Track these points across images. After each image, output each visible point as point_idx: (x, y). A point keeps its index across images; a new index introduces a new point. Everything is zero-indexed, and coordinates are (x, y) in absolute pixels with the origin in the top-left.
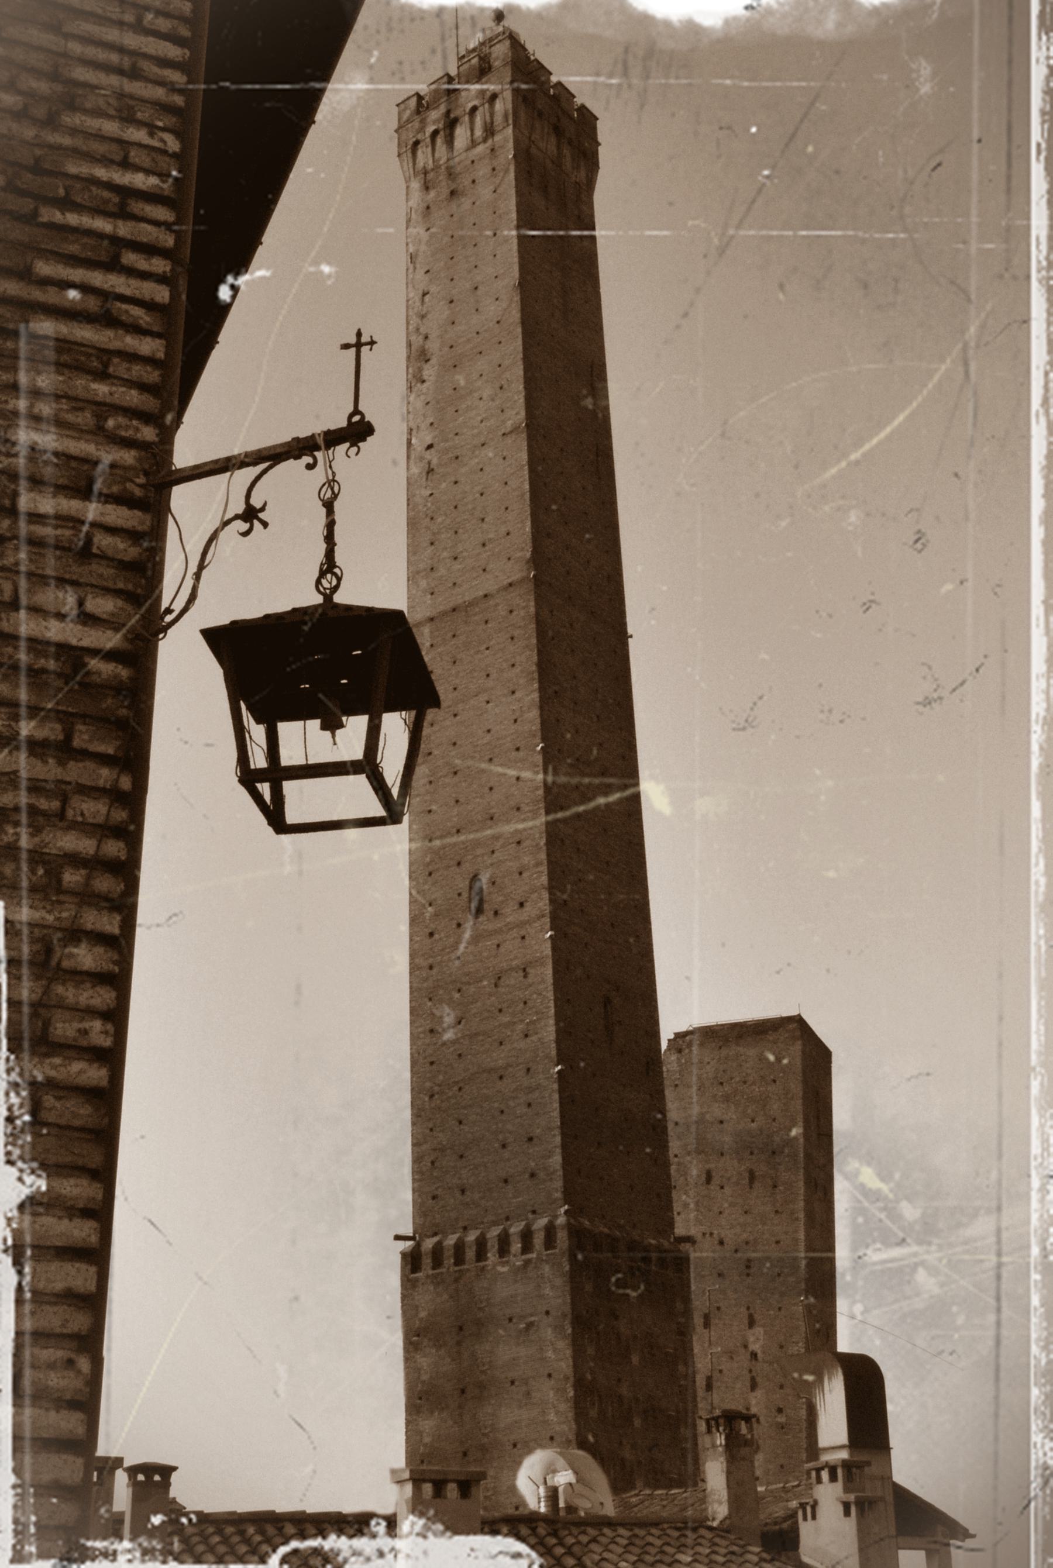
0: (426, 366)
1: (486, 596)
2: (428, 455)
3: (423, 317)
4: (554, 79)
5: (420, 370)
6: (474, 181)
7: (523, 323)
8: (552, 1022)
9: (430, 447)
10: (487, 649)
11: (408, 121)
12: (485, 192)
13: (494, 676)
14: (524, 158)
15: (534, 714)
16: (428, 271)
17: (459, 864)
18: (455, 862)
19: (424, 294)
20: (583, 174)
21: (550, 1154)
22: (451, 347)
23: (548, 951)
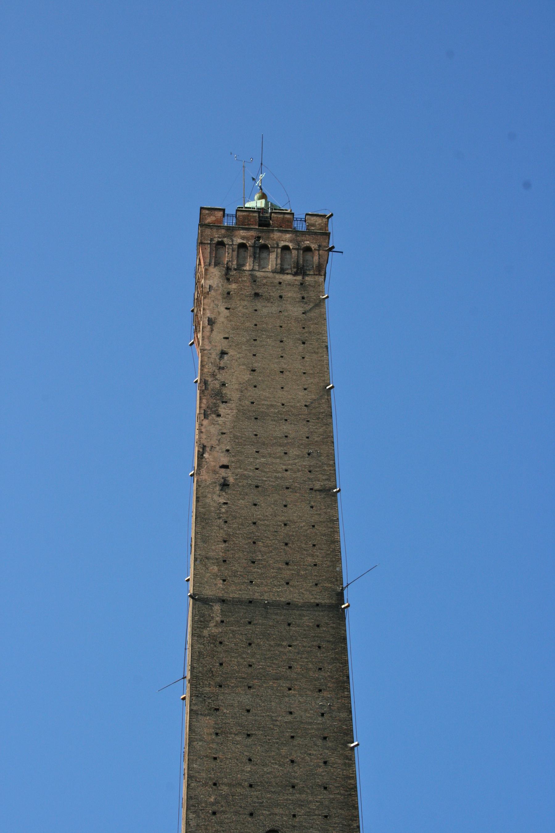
0: (223, 406)
1: (289, 604)
3: (221, 368)
5: (216, 405)
10: (290, 646)
13: (297, 668)
16: (227, 338)
17: (251, 814)
18: (247, 812)
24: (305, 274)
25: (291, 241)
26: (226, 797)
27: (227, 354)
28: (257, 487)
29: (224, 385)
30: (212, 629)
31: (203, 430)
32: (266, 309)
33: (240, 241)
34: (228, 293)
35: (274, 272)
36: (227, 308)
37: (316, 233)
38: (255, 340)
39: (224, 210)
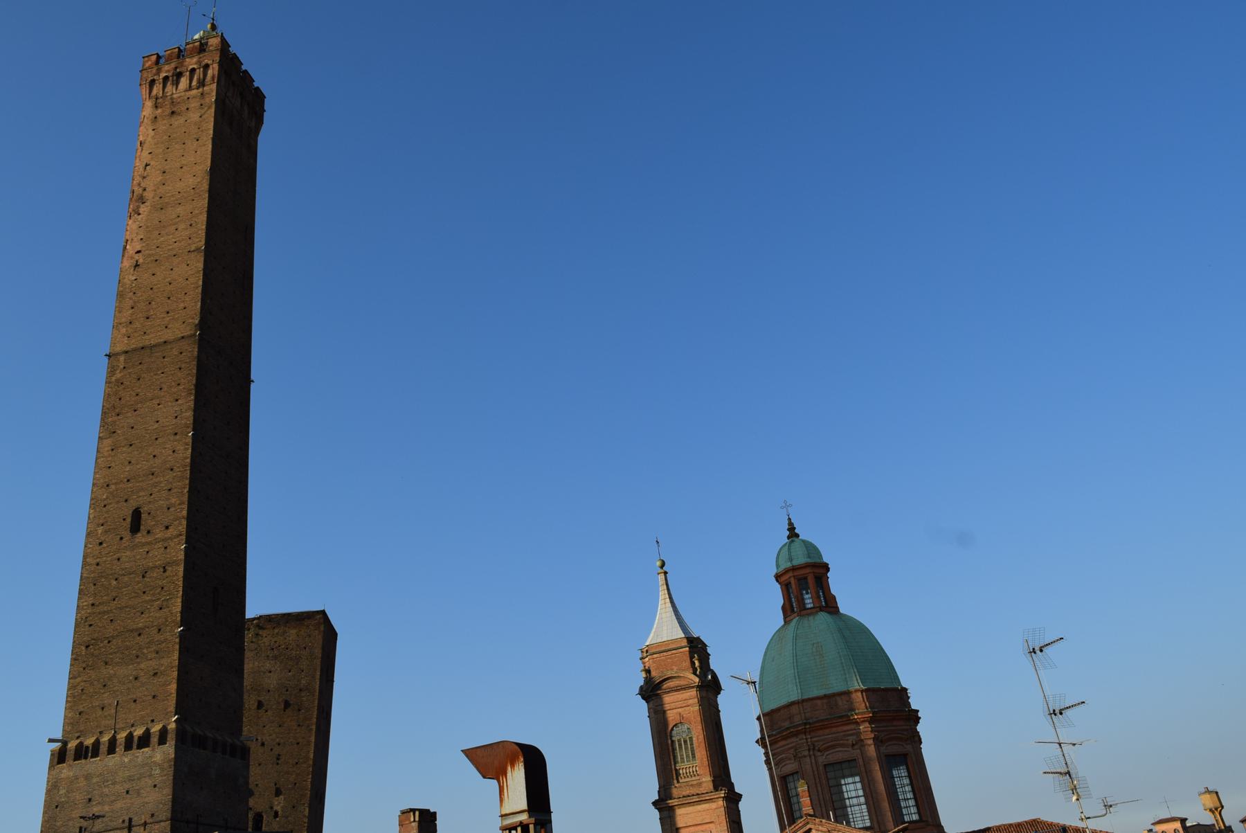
2: (137, 257)
4: (244, 68)
5: (138, 207)
7: (210, 191)
8: (179, 600)
9: (139, 252)
11: (150, 68)
12: (194, 116)
13: (165, 388)
14: (221, 104)
15: (190, 414)
20: (253, 124)
21: (166, 684)
23: (182, 556)
26: (111, 493)
30: (118, 375)
32: (178, 121)
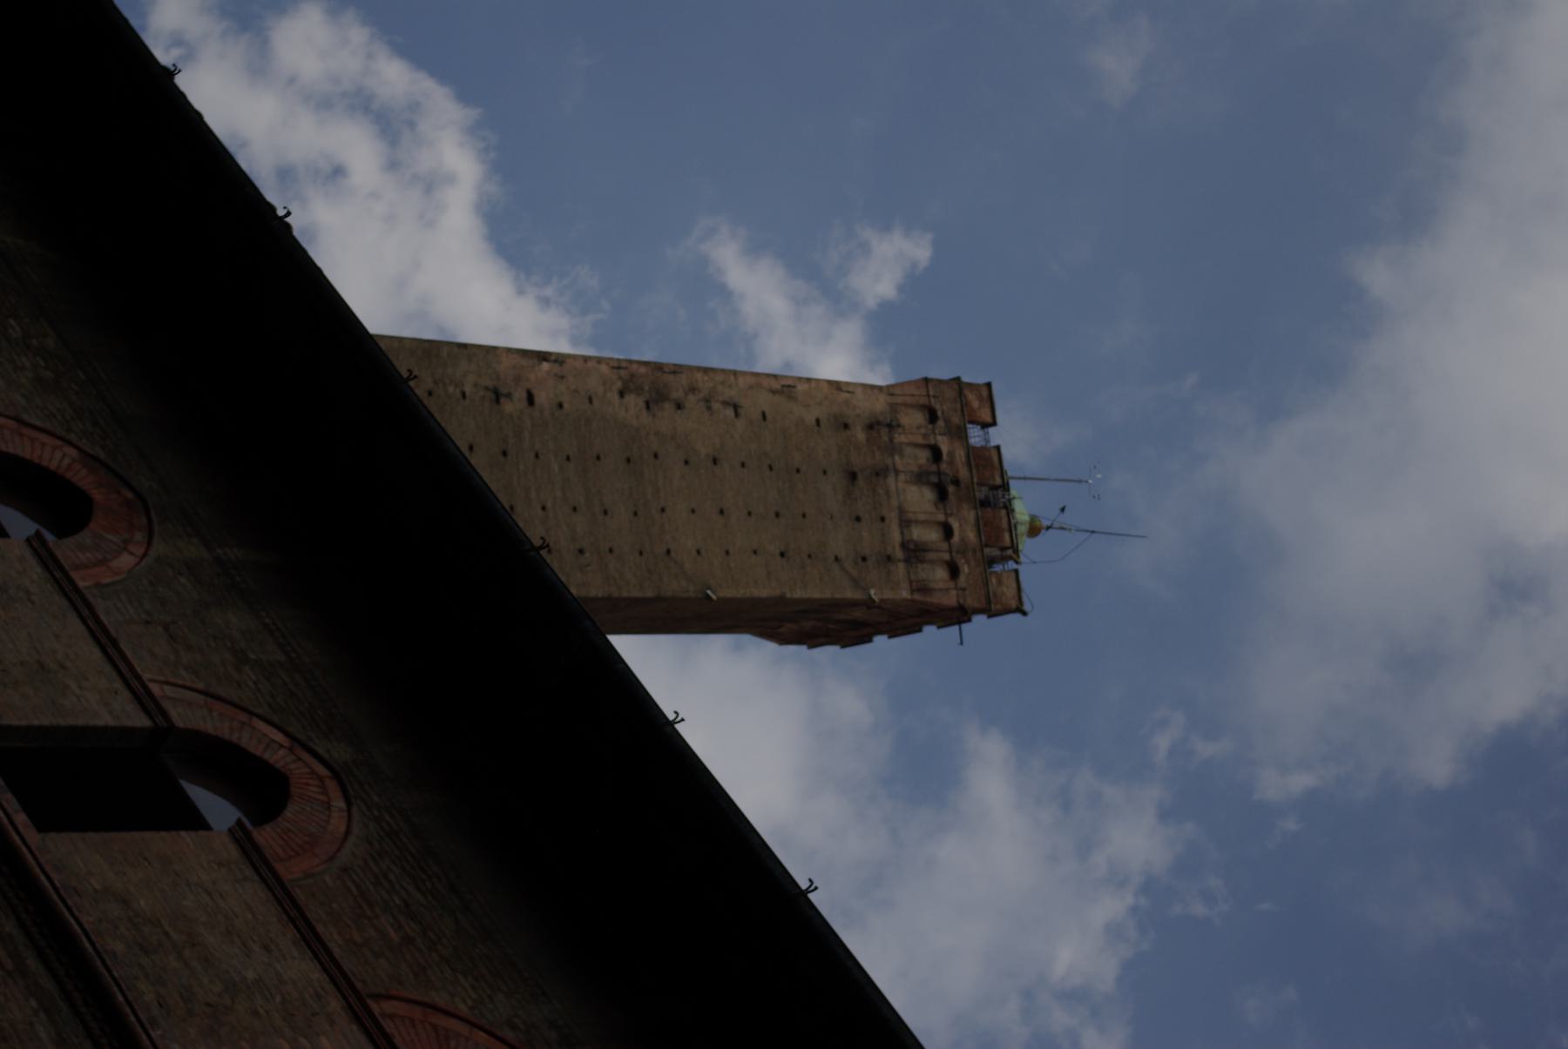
0: (641, 402)
2: (520, 394)
3: (707, 401)
5: (639, 390)
6: (858, 519)
9: (530, 399)
16: (764, 417)
19: (736, 407)
22: (656, 456)
24: (907, 561)
25: (962, 540)
27: (737, 415)
28: (505, 454)
29: (679, 406)
31: (590, 364)
33: (944, 449)
34: (846, 426)
35: (902, 511)
36: (818, 421)
37: (986, 584)
38: (771, 468)
39: (994, 423)
